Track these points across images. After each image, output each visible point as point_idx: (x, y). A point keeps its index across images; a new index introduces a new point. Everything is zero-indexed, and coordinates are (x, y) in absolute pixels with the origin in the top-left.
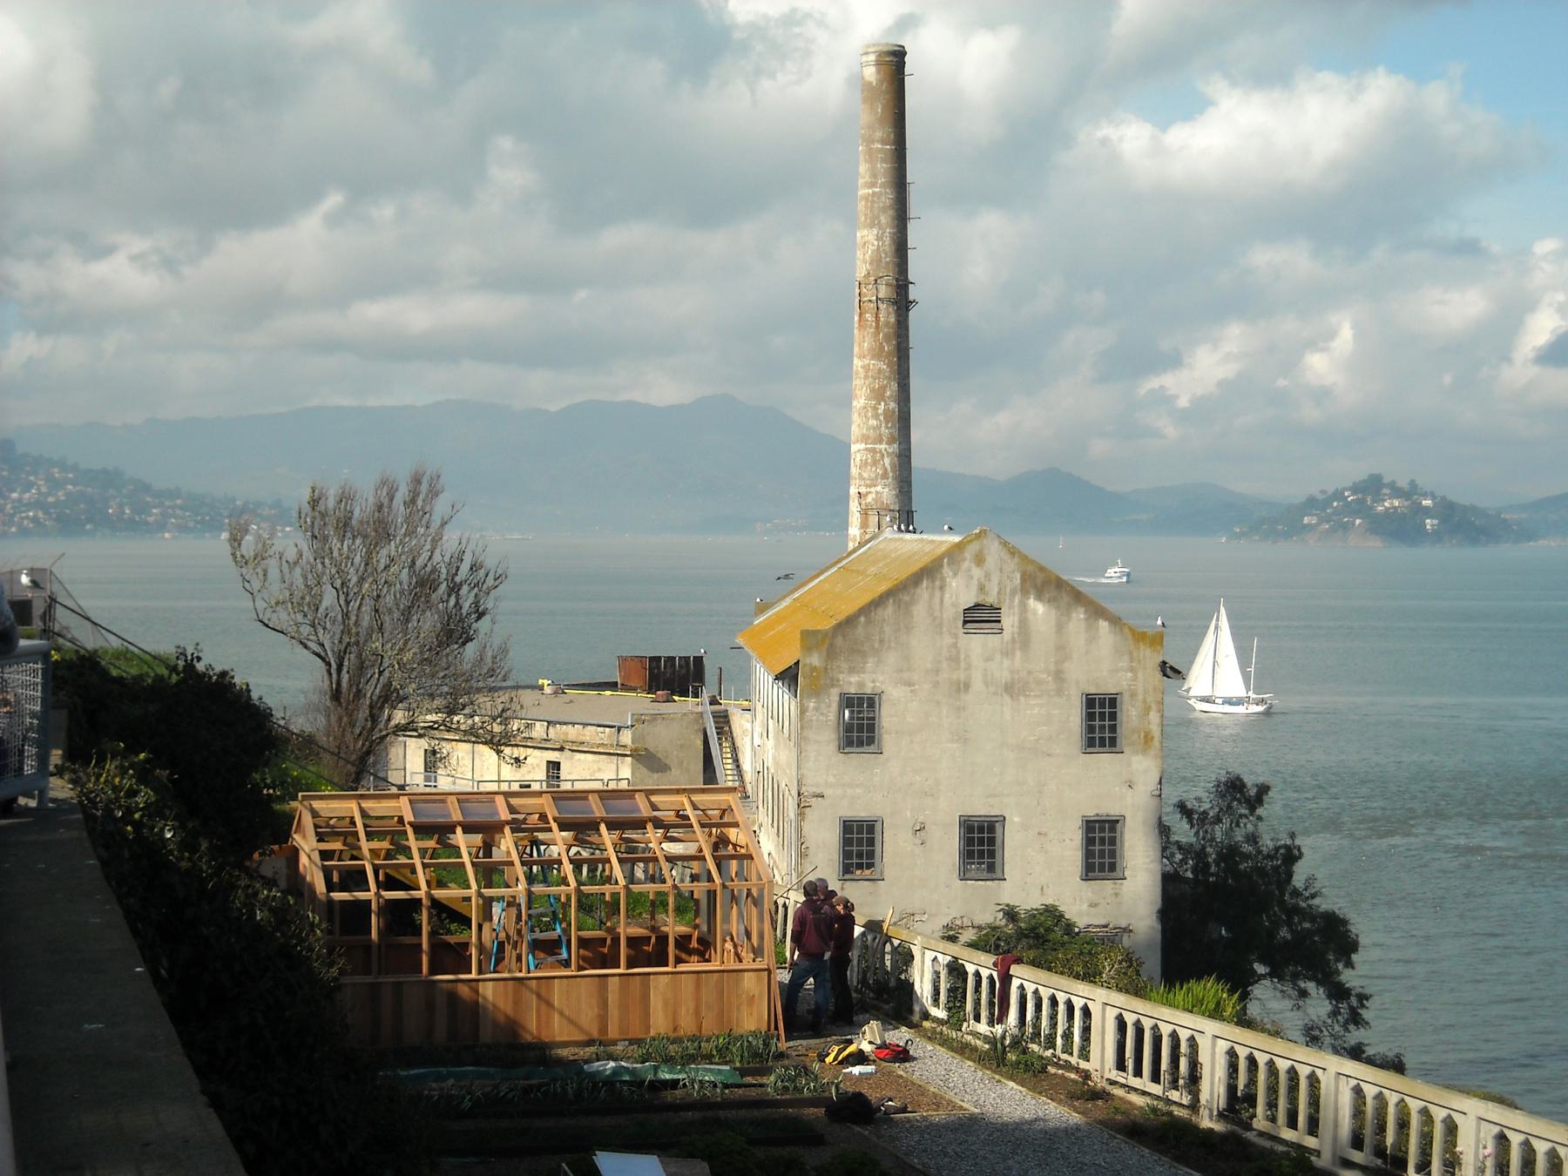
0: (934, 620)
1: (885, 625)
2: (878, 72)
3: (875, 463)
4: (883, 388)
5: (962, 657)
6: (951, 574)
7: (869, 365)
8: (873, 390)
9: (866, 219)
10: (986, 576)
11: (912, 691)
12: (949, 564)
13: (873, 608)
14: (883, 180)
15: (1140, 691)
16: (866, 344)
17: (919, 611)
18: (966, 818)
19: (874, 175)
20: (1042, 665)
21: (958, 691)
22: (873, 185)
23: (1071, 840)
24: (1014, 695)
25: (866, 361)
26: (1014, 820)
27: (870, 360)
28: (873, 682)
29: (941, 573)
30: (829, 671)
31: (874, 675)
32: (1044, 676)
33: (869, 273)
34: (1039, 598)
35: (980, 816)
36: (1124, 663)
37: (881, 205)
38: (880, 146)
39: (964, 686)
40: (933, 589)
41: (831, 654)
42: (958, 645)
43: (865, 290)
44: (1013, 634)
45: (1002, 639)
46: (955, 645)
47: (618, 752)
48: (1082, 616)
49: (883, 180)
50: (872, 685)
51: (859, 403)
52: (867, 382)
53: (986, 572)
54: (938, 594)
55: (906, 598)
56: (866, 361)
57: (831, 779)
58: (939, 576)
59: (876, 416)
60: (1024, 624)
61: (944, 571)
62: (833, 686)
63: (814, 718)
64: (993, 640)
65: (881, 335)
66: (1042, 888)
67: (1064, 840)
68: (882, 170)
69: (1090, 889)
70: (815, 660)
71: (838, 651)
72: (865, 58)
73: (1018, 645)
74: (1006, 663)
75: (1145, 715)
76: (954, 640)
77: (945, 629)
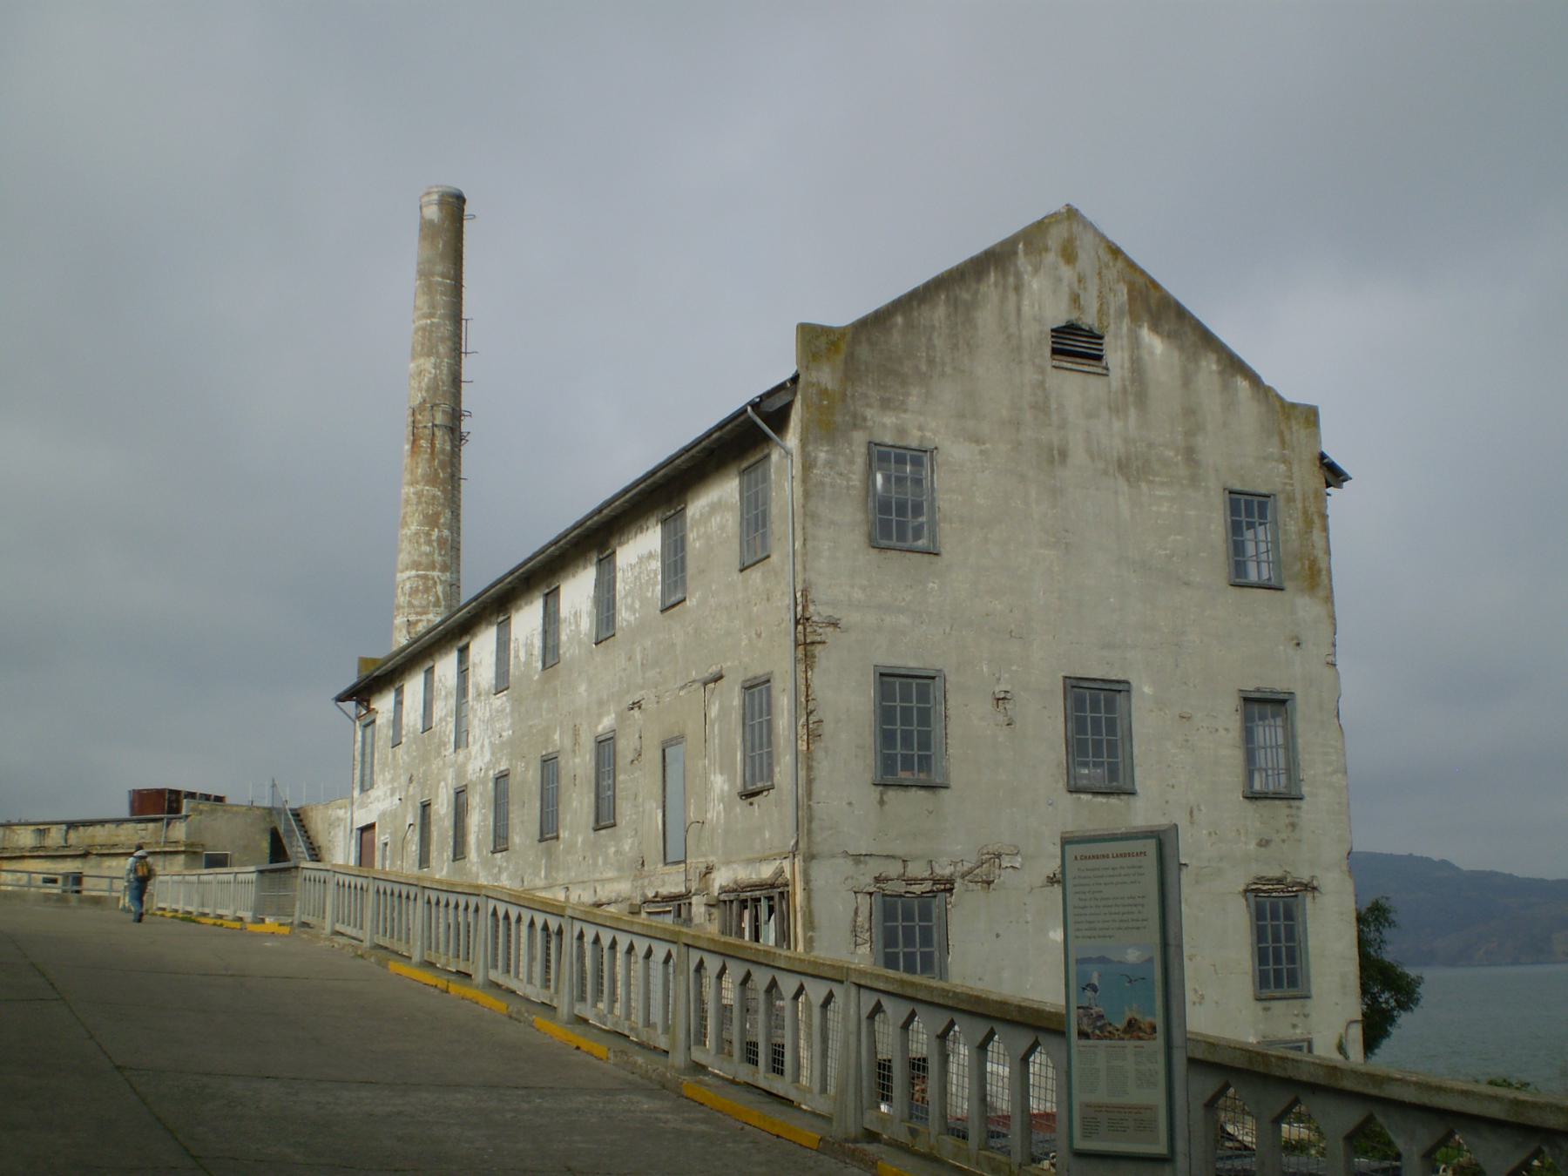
0: (1009, 337)
1: (935, 335)
2: (441, 210)
3: (427, 590)
4: (437, 515)
5: (1054, 406)
6: (1029, 268)
7: (422, 491)
8: (426, 516)
9: (422, 349)
10: (1080, 281)
11: (982, 452)
12: (1026, 254)
13: (915, 304)
14: (442, 311)
15: (1298, 496)
16: (420, 470)
17: (986, 317)
18: (1075, 683)
19: (433, 306)
20: (1168, 436)
21: (1051, 461)
22: (431, 315)
23: (1227, 730)
24: (1132, 479)
25: (419, 487)
26: (1144, 689)
27: (424, 486)
28: (921, 428)
29: (1016, 265)
30: (849, 400)
31: (922, 419)
32: (1171, 454)
33: (424, 401)
34: (1155, 328)
35: (1094, 680)
36: (1274, 449)
37: (440, 335)
38: (440, 279)
39: (1060, 454)
40: (1005, 288)
41: (852, 371)
42: (1047, 385)
43: (419, 417)
44: (1123, 379)
45: (1109, 385)
46: (1041, 384)
47: (167, 849)
48: (1214, 367)
49: (442, 311)
50: (920, 433)
51: (409, 529)
52: (420, 508)
53: (1079, 275)
54: (1012, 297)
55: (966, 296)
56: (419, 487)
57: (858, 595)
58: (1012, 269)
59: (429, 543)
60: (1137, 368)
61: (1019, 263)
62: (855, 426)
63: (828, 480)
64: (1095, 385)
65: (436, 461)
66: (1191, 812)
67: (1217, 730)
68: (442, 302)
69: (1257, 815)
70: (826, 376)
71: (863, 368)
72: (425, 199)
73: (1131, 399)
74: (1117, 425)
75: (1306, 532)
76: (1040, 378)
77: (1026, 356)
